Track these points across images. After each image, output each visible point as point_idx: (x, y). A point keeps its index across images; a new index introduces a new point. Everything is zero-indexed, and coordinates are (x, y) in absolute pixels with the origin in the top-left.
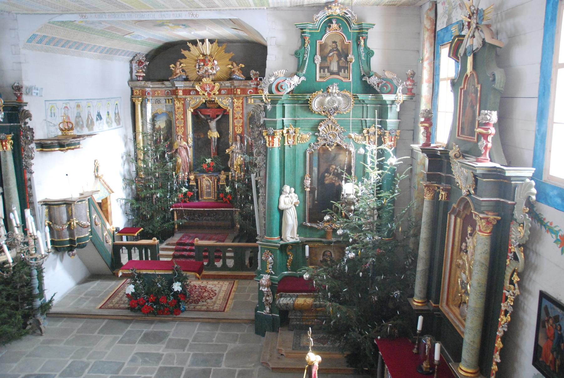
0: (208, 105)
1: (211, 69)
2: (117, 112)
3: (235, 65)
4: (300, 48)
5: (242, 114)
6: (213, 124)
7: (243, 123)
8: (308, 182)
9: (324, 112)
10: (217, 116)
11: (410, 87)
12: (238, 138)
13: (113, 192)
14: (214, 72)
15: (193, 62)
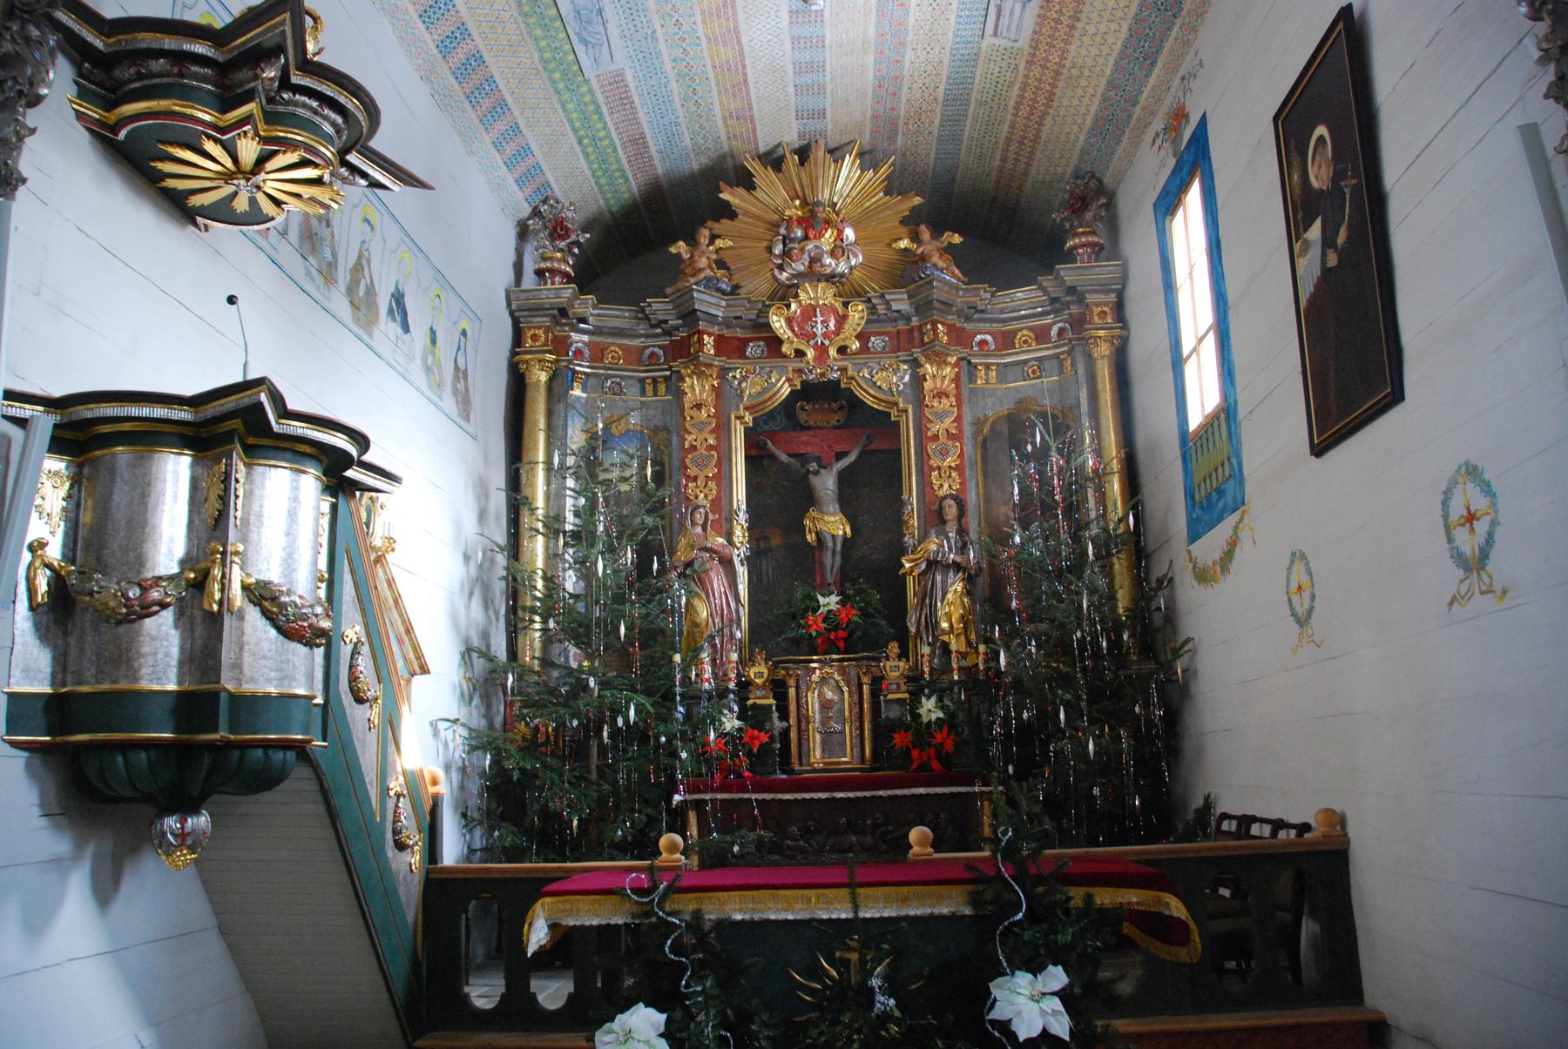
0: (802, 417)
1: (832, 254)
2: (462, 366)
3: (926, 234)
5: (958, 419)
6: (826, 483)
7: (961, 456)
10: (840, 456)
12: (951, 510)
13: (425, 670)
14: (842, 268)
15: (761, 230)
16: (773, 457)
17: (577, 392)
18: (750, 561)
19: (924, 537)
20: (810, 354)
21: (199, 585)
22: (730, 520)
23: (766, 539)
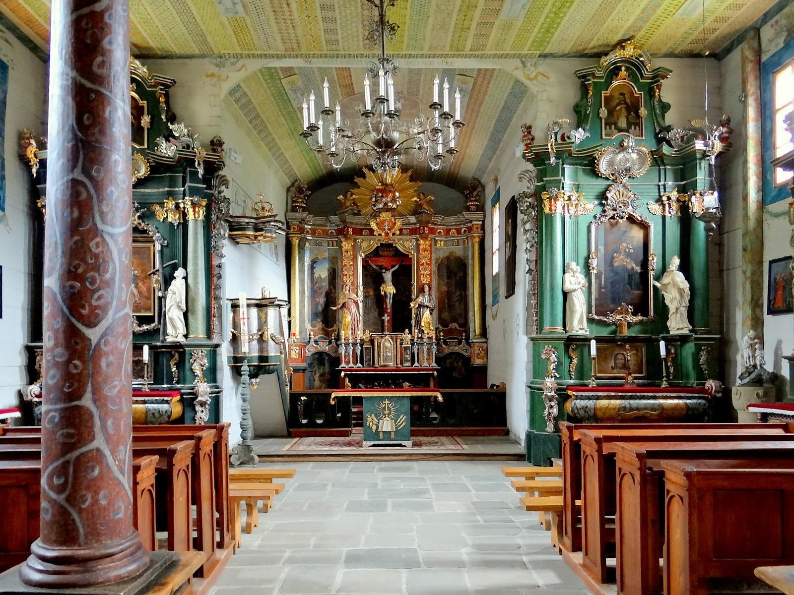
0: (381, 253)
3: (422, 196)
4: (582, 98)
5: (430, 258)
6: (388, 276)
7: (431, 270)
8: (594, 263)
9: (613, 174)
10: (393, 266)
11: (727, 135)
14: (395, 206)
16: (370, 265)
17: (307, 245)
18: (364, 302)
19: (417, 297)
20: (383, 234)
21: (261, 336)
22: (357, 288)
23: (368, 292)
